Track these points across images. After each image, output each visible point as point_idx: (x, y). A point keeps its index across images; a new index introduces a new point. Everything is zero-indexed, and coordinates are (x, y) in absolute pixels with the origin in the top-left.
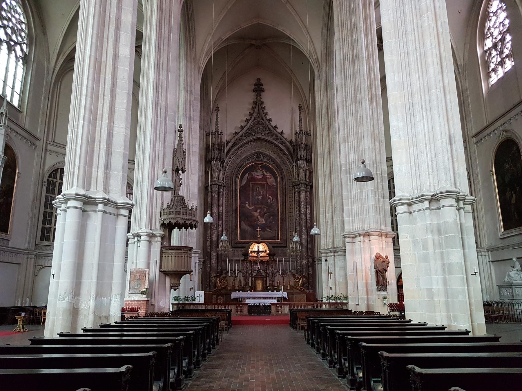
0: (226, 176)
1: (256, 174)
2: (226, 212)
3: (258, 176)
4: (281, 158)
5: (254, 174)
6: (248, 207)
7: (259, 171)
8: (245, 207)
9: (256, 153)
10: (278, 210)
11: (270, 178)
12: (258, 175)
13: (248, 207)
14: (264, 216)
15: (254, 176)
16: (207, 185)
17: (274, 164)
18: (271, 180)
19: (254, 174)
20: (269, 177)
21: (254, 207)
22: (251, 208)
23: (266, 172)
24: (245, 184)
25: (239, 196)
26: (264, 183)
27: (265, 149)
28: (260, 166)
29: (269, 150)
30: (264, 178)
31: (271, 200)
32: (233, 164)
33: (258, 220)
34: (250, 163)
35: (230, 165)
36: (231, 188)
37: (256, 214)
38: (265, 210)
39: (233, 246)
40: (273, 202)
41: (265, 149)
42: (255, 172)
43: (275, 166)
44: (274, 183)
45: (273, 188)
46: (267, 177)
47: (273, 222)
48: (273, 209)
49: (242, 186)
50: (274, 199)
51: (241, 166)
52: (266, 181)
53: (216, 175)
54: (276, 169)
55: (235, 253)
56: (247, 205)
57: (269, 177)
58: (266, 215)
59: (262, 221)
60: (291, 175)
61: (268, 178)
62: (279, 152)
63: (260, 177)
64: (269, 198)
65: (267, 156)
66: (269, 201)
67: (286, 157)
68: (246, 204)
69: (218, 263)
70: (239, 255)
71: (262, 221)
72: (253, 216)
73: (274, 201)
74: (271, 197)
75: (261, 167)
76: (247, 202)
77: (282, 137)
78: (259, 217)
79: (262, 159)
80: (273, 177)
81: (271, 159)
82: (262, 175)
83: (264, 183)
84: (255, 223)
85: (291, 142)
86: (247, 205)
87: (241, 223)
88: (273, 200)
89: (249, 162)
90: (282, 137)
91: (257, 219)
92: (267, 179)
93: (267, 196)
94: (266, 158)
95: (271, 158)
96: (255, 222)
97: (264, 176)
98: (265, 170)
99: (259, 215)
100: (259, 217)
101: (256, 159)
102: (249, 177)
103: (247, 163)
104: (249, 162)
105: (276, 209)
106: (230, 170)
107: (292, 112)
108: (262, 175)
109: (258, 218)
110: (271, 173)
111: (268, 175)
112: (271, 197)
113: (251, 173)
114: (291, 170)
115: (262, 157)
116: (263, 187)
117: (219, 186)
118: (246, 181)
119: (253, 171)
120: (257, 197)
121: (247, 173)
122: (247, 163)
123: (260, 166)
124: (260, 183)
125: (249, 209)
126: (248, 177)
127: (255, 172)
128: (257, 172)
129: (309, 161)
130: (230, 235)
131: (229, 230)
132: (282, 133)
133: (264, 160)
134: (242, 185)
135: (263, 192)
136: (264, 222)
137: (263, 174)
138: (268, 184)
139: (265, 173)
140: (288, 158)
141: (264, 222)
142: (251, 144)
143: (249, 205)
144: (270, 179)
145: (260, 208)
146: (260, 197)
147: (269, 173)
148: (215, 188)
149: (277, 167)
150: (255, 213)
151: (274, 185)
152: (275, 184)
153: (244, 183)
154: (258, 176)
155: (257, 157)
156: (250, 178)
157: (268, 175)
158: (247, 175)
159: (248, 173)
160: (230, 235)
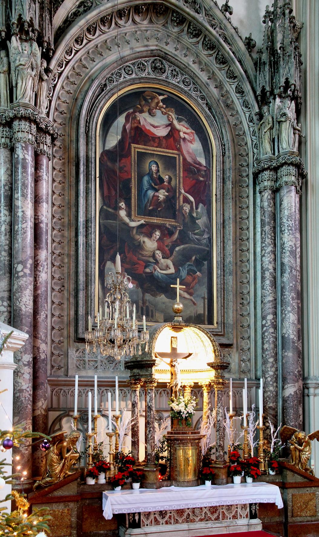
0: (56, 109)
1: (150, 120)
2: (57, 227)
3: (155, 127)
6: (127, 220)
7: (158, 112)
8: (116, 217)
9: (152, 54)
10: (210, 239)
11: (191, 142)
13: (127, 220)
14: (172, 251)
15: (144, 125)
17: (203, 98)
20: (186, 136)
21: (142, 222)
22: (133, 224)
23: (180, 120)
24: (116, 147)
25: (98, 179)
26: (171, 153)
27: (176, 49)
28: (161, 98)
29: (186, 56)
31: (192, 207)
32: (78, 74)
33: (157, 262)
34: (133, 82)
35: (68, 77)
36: (73, 153)
38: (176, 235)
39: (81, 336)
40: (197, 213)
41: (176, 49)
42: (146, 115)
43: (204, 106)
44: (201, 157)
45: (199, 170)
46: (182, 134)
47: (198, 273)
48: (195, 234)
49: (108, 151)
50: (201, 205)
51: (105, 85)
52: (179, 150)
54: (207, 117)
55: (87, 359)
56: (123, 213)
57: (186, 136)
58: (177, 249)
59: (168, 267)
60: (246, 144)
61: (184, 139)
62: (215, 67)
63: (162, 132)
64: (186, 200)
66: (187, 208)
67: (234, 87)
68: (120, 208)
69: (35, 387)
70: (99, 364)
72: (140, 247)
73: (199, 210)
74: (192, 199)
75: (163, 101)
76: (122, 205)
77: (225, 22)
78: (159, 254)
79: (167, 77)
80: (196, 136)
81: (194, 84)
82: (167, 126)
83: (171, 153)
84: (148, 270)
85: (249, 44)
86: (123, 213)
87: (104, 266)
88: (197, 208)
89: (128, 77)
90: (225, 22)
91: (152, 260)
92: (181, 140)
93: (180, 193)
94: (179, 77)
96: (146, 267)
97: (173, 133)
98: (176, 113)
99: (158, 249)
100: (159, 254)
101: (149, 74)
102: (128, 126)
103: (122, 80)
104: (128, 77)
105: (206, 236)
106: (68, 92)
108: (167, 126)
109: (154, 256)
110: (188, 122)
111: (183, 128)
112: (192, 199)
113: (135, 118)
114: (246, 128)
115: (168, 72)
116: (170, 163)
118: (119, 137)
119: (142, 112)
120: (151, 193)
121: (121, 113)
122: (122, 80)
123: (161, 98)
125: (127, 225)
126: (124, 126)
127: (146, 115)
130: (68, 300)
131: (66, 285)
133: (174, 81)
134: (107, 148)
135: (170, 179)
136: (172, 270)
137: (171, 125)
138: (185, 159)
139: (175, 122)
140: (240, 91)
141: (172, 270)
142: (134, 21)
143: (129, 215)
144: (189, 144)
146: (162, 195)
147: (186, 125)
149: (210, 109)
150: (146, 240)
151: (200, 164)
152: (203, 161)
153: (113, 141)
154: (155, 127)
155: (155, 68)
156: (131, 129)
157: (185, 130)
158: (121, 120)
159: (125, 114)
160: (68, 300)
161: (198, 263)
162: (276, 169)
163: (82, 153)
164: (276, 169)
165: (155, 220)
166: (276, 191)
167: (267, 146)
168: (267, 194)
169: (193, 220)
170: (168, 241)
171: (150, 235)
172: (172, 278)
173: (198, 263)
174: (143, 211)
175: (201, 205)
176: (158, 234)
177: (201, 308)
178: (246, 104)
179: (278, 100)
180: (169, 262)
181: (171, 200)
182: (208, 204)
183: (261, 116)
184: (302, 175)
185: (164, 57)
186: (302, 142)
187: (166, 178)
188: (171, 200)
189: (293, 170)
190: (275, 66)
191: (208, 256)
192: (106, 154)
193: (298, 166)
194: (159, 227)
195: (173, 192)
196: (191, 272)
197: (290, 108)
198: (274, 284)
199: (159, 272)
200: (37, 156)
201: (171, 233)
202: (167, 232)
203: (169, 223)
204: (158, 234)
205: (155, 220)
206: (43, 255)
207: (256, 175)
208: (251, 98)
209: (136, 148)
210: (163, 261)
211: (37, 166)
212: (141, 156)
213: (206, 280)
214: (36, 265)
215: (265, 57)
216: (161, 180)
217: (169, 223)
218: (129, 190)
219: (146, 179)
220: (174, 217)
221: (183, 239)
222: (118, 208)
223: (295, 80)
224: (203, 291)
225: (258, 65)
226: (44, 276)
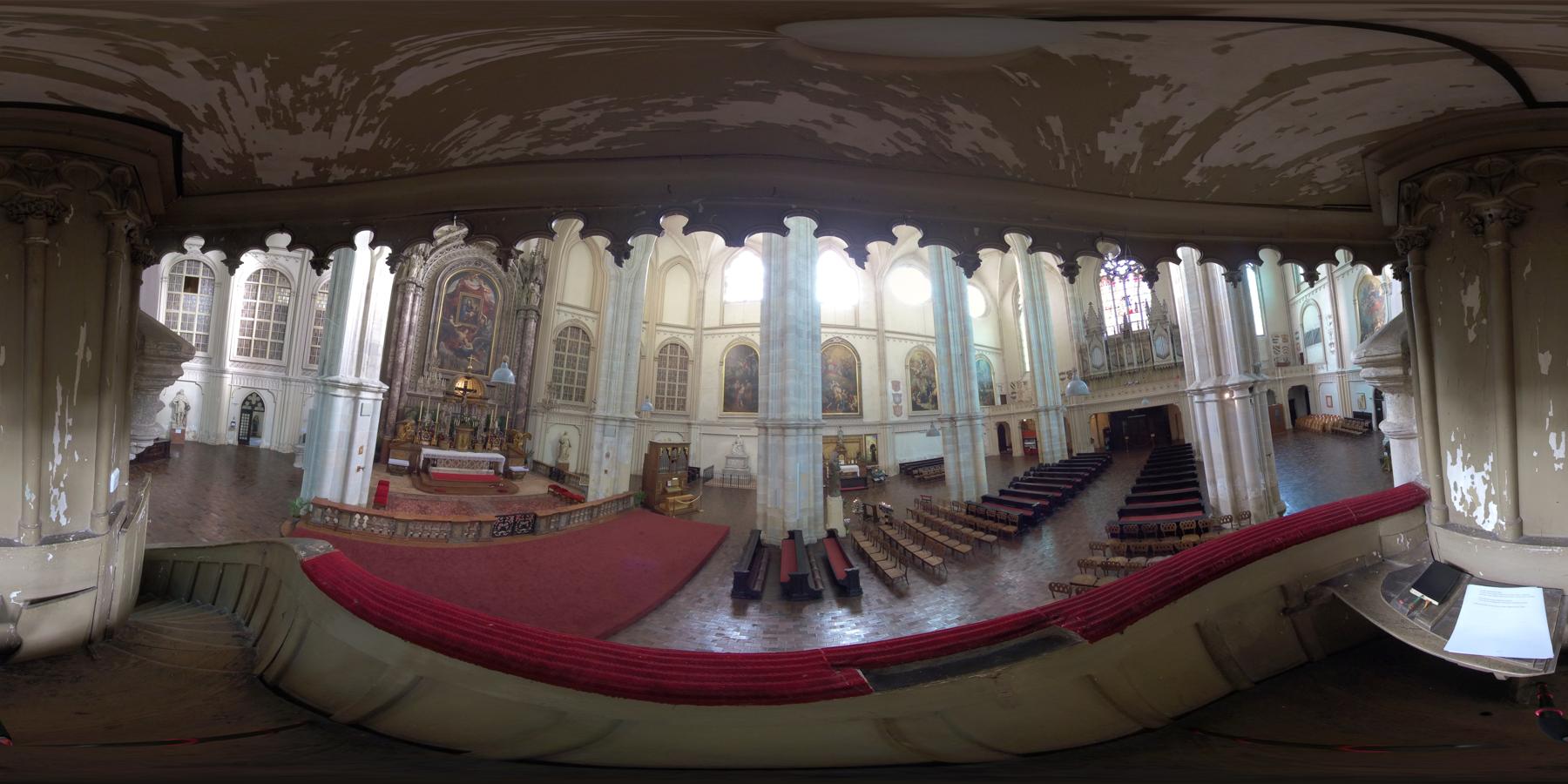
1: (471, 283)
5: (468, 282)
10: (492, 336)
12: (474, 284)
14: (473, 339)
16: (398, 283)
18: (490, 296)
19: (468, 282)
30: (481, 289)
37: (463, 335)
42: (469, 281)
50: (490, 321)
52: (483, 296)
53: (415, 271)
56: (451, 321)
59: (469, 347)
63: (476, 288)
64: (483, 317)
65: (489, 265)
71: (469, 347)
72: (458, 336)
78: (466, 340)
86: (451, 321)
100: (466, 340)
111: (486, 288)
116: (478, 301)
117: (417, 286)
118: (454, 288)
124: (474, 296)
128: (472, 280)
129: (542, 289)
136: (472, 348)
141: (472, 348)
145: (469, 328)
146: (471, 314)
148: (412, 288)
150: (461, 333)
153: (452, 290)
155: (476, 264)
158: (457, 282)
161: (485, 346)
162: (527, 311)
163: (436, 294)
164: (527, 311)
166: (525, 320)
167: (524, 300)
168: (521, 321)
169: (485, 326)
170: (471, 335)
171: (463, 331)
172: (470, 353)
173: (485, 346)
174: (460, 320)
175: (490, 321)
176: (467, 331)
177: (483, 367)
179: (532, 284)
180: (471, 345)
181: (476, 317)
182: (493, 320)
183: (523, 288)
184: (539, 315)
185: (481, 260)
186: (541, 301)
187: (474, 307)
188: (476, 317)
189: (534, 313)
190: (532, 271)
191: (490, 344)
192: (446, 295)
194: (467, 328)
195: (477, 313)
196: (481, 350)
197: (537, 289)
198: (519, 360)
199: (465, 348)
200: (415, 296)
201: (473, 331)
202: (472, 331)
203: (473, 326)
204: (467, 331)
206: (412, 337)
209: (462, 294)
210: (468, 344)
211: (414, 300)
212: (464, 297)
213: (487, 354)
214: (408, 341)
215: (528, 267)
216: (472, 308)
217: (473, 326)
218: (456, 311)
219: (465, 307)
220: (476, 324)
221: (479, 334)
222: (450, 318)
223: (541, 277)
224: (486, 359)
225: (525, 269)
226: (411, 347)
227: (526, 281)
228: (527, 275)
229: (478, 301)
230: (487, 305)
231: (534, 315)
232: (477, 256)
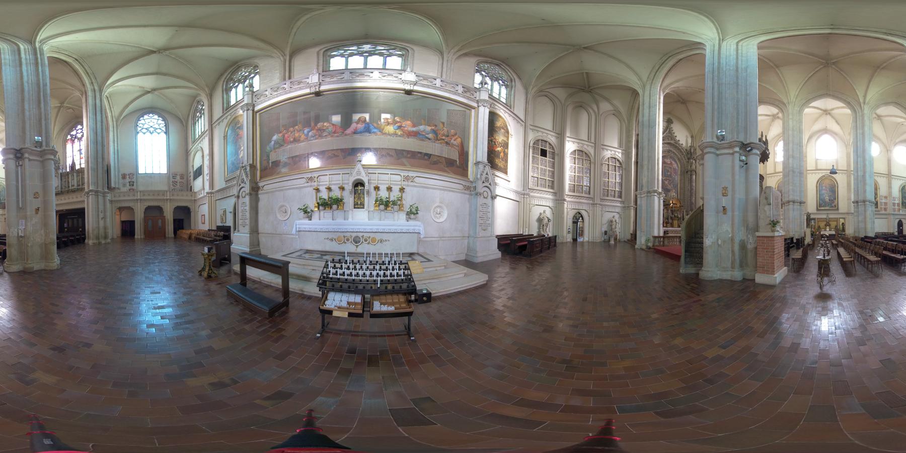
4: (680, 156)
18: (675, 166)
63: (669, 162)
85: (686, 150)
95: (676, 154)
97: (671, 163)
107: (687, 137)
111: (673, 162)
116: (670, 168)
132: (682, 144)
140: (684, 157)
162: (691, 171)
164: (691, 171)
165: (667, 178)
166: (691, 175)
178: (685, 159)
181: (670, 175)
183: (688, 162)
184: (696, 173)
188: (670, 175)
193: (696, 171)
197: (694, 162)
203: (671, 179)
205: (667, 178)
207: (687, 172)
208: (686, 158)
215: (689, 152)
227: (689, 159)
228: (689, 156)
229: (670, 168)
230: (675, 169)
231: (694, 173)
232: (667, 149)
